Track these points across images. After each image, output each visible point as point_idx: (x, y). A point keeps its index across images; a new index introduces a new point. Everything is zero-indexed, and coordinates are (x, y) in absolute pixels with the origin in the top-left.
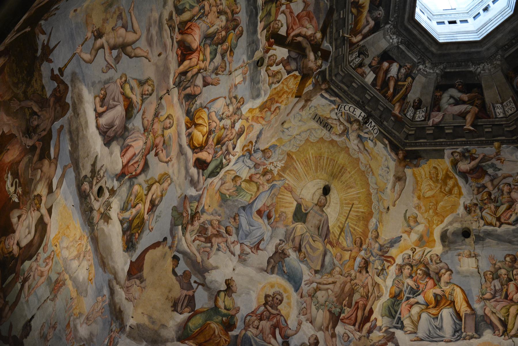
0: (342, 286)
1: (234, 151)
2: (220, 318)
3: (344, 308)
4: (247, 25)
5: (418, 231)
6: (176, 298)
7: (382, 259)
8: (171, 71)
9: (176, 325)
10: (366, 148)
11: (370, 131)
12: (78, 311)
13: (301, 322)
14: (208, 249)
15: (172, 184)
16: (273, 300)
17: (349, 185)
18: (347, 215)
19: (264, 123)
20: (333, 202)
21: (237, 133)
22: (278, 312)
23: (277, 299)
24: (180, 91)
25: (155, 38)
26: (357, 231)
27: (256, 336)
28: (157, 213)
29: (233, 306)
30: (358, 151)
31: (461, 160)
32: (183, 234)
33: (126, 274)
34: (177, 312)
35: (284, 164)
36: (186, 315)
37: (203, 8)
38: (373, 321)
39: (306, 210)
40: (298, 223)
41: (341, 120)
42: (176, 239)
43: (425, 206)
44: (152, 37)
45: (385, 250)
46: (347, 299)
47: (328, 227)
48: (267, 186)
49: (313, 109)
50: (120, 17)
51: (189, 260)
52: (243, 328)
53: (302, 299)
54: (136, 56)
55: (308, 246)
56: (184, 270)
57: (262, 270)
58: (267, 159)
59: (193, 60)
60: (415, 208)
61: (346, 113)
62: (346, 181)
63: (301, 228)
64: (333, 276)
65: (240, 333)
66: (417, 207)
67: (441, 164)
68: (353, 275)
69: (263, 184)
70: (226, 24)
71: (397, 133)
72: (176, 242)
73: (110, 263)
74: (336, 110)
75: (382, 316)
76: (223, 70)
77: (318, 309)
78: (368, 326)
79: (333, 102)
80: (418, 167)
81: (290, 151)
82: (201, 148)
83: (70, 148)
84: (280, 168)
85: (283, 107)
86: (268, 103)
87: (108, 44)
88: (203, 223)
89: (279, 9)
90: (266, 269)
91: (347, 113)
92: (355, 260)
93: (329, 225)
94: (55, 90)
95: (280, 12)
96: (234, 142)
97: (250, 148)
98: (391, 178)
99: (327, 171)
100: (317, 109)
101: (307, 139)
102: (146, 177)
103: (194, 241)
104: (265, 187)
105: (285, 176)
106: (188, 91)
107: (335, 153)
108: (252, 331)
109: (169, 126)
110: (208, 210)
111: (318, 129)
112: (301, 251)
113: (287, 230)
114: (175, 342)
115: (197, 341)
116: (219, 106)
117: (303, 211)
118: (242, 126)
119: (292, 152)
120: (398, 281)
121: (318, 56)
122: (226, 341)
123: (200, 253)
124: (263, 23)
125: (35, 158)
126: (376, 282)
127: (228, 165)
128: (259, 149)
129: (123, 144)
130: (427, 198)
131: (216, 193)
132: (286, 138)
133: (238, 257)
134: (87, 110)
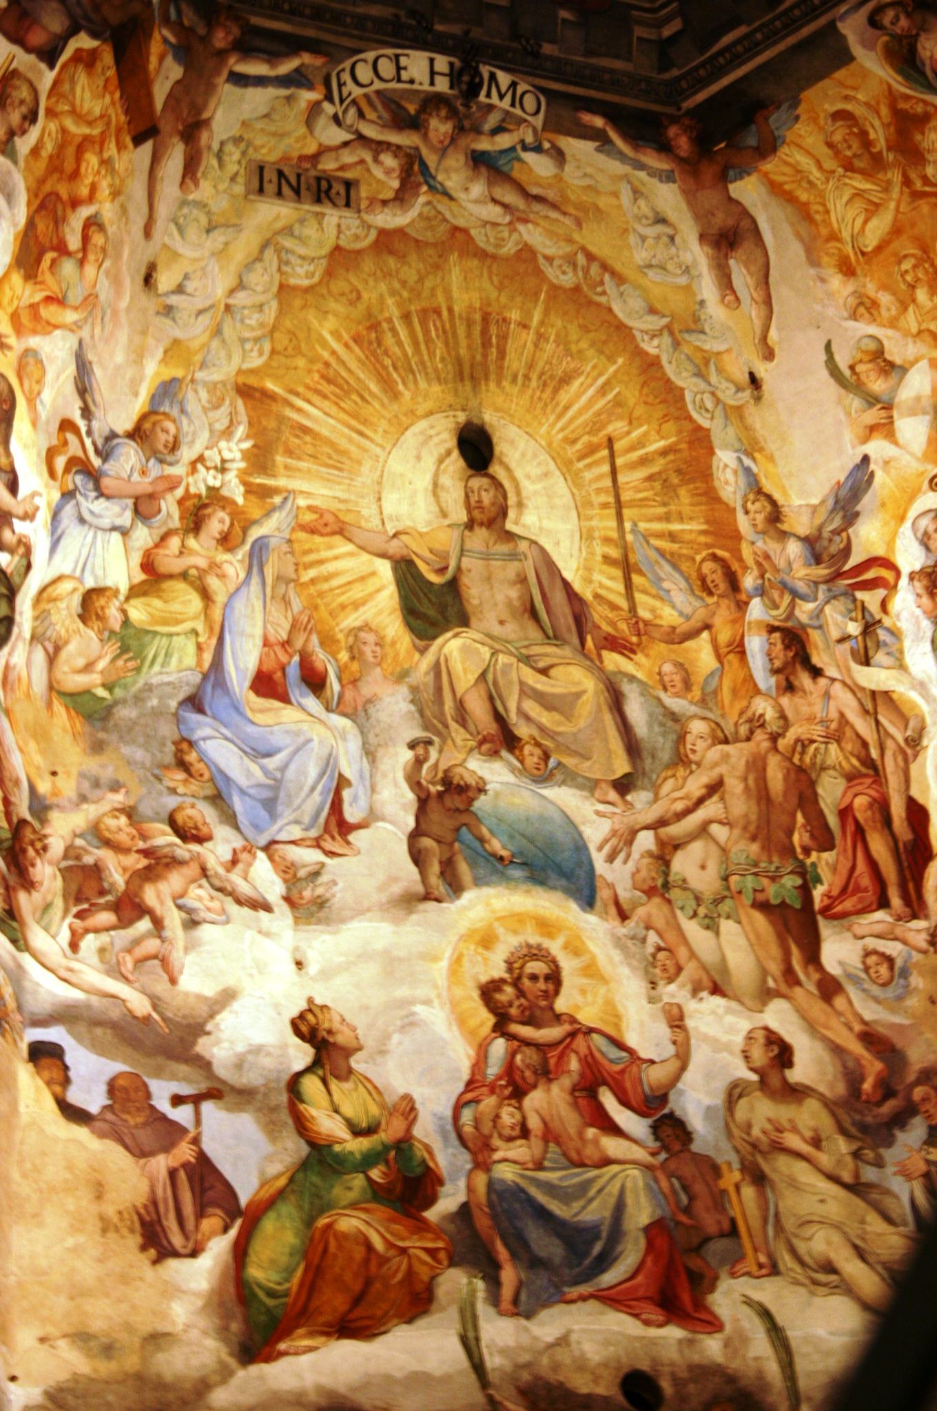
0: (751, 782)
2: (358, 1181)
3: (808, 862)
5: (918, 399)
6: (139, 1204)
7: (842, 589)
9: (205, 1307)
10: (535, 191)
11: (507, 113)
13: (675, 1011)
14: (152, 945)
16: (521, 993)
17: (552, 377)
18: (611, 500)
19: (70, 317)
20: (528, 477)
23: (534, 978)
26: (687, 537)
27: (539, 1166)
29: (383, 1106)
30: (508, 219)
31: (923, 28)
32: (14, 941)
34: (176, 1254)
35: (248, 437)
36: (218, 1248)
39: (442, 571)
40: (440, 640)
41: (370, 131)
43: (884, 287)
45: (834, 549)
46: (800, 818)
47: (566, 585)
48: (234, 564)
49: (233, 154)
51: (99, 1031)
53: (631, 923)
55: (531, 707)
57: (411, 901)
58: (169, 458)
60: (854, 316)
61: (374, 97)
62: (531, 366)
63: (465, 650)
64: (698, 764)
65: (470, 1189)
66: (862, 310)
67: (855, 88)
68: (770, 714)
69: (214, 566)
71: (618, 65)
74: (329, 109)
77: (711, 925)
79: (297, 80)
80: (773, 149)
81: (240, 372)
84: (243, 465)
85: (107, 210)
86: (41, 226)
88: (70, 851)
90: (420, 889)
91: (378, 92)
92: (743, 653)
93: (568, 575)
97: (74, 448)
98: (697, 255)
99: (436, 370)
100: (249, 144)
101: (282, 287)
103: (74, 946)
104: (230, 570)
105: (281, 482)
107: (421, 280)
108: (511, 1154)
111: (302, 221)
112: (519, 739)
113: (414, 690)
115: (322, 1319)
117: (434, 578)
122: (431, 1252)
123: (127, 980)
126: (873, 693)
127: (29, 566)
128: (113, 435)
130: (879, 249)
131: (49, 705)
132: (195, 331)
133: (285, 907)
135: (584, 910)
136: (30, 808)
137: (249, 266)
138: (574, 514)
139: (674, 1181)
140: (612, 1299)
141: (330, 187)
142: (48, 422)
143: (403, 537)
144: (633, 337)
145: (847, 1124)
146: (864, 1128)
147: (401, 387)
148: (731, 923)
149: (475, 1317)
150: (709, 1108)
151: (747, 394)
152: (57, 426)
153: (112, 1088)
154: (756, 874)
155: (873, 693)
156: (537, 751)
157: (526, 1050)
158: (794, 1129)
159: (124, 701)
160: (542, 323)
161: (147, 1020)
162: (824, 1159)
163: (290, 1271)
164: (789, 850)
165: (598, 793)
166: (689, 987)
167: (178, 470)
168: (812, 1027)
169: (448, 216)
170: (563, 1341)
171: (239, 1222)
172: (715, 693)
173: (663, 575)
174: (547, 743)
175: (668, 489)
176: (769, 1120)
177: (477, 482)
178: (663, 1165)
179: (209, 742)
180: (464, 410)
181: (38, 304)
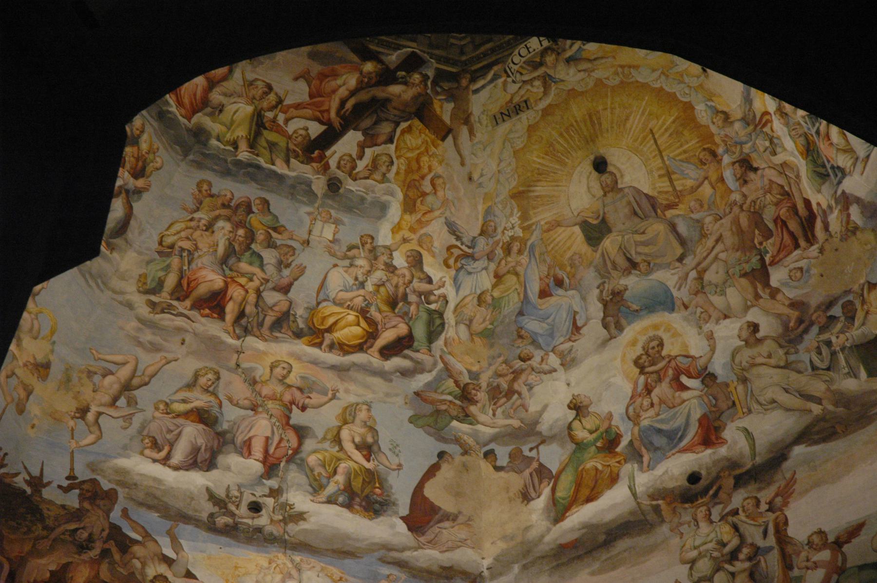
0: (734, 229)
1: (434, 283)
3: (762, 247)
4: (262, 189)
6: (521, 489)
8: (218, 335)
10: (592, 57)
13: (710, 333)
14: (519, 402)
19: (437, 213)
22: (667, 360)
23: (653, 348)
24: (258, 333)
25: (158, 339)
27: (658, 415)
32: (471, 424)
33: (410, 533)
34: (533, 499)
35: (518, 211)
36: (547, 491)
37: (182, 250)
38: (818, 211)
40: (602, 244)
42: (465, 437)
44: (151, 343)
45: (751, 117)
46: (757, 232)
47: (646, 195)
48: (524, 259)
50: (90, 374)
53: (690, 309)
54: (152, 376)
55: (641, 249)
56: (508, 453)
57: (604, 343)
59: (235, 294)
62: (612, 123)
65: (632, 434)
69: (518, 263)
70: (232, 223)
72: (471, 441)
73: (358, 545)
74: (509, 80)
75: (819, 191)
76: (291, 253)
77: (723, 293)
78: (819, 225)
81: (510, 190)
82: (372, 335)
83: (156, 515)
84: (519, 222)
85: (439, 169)
86: (411, 194)
87: (104, 405)
89: (279, 125)
90: (608, 337)
91: (524, 62)
93: (645, 192)
94: (80, 495)
95: (284, 126)
96: (419, 278)
97: (456, 252)
101: (514, 152)
102: (317, 437)
103: (494, 415)
104: (523, 261)
105: (534, 220)
106: (269, 321)
107: (562, 118)
108: (647, 416)
109: (285, 372)
113: (595, 267)
114: (554, 528)
117: (595, 222)
118: (409, 253)
119: (514, 188)
120: (793, 130)
121: (402, 78)
122: (618, 462)
123: (512, 418)
125: (117, 557)
127: (447, 302)
128: (474, 238)
131: (472, 340)
133: (562, 368)
134: (143, 472)
135: (670, 313)
136: (470, 379)
138: (644, 166)
139: (711, 397)
140: (684, 450)
141: (520, 106)
142: (440, 252)
143: (582, 214)
144: (649, 86)
145: (784, 343)
146: (790, 341)
147: (567, 160)
148: (731, 288)
149: (634, 477)
150: (724, 364)
151: (703, 77)
153: (510, 456)
154: (740, 264)
155: (781, 164)
158: (760, 355)
159: (498, 326)
160: (612, 103)
161: (520, 427)
162: (773, 361)
163: (570, 489)
164: (755, 247)
165: (671, 267)
166: (715, 321)
167: (499, 237)
168: (766, 312)
169: (565, 88)
170: (667, 471)
171: (553, 480)
172: (714, 202)
174: (649, 259)
175: (678, 133)
176: (749, 357)
178: (705, 394)
180: (592, 154)
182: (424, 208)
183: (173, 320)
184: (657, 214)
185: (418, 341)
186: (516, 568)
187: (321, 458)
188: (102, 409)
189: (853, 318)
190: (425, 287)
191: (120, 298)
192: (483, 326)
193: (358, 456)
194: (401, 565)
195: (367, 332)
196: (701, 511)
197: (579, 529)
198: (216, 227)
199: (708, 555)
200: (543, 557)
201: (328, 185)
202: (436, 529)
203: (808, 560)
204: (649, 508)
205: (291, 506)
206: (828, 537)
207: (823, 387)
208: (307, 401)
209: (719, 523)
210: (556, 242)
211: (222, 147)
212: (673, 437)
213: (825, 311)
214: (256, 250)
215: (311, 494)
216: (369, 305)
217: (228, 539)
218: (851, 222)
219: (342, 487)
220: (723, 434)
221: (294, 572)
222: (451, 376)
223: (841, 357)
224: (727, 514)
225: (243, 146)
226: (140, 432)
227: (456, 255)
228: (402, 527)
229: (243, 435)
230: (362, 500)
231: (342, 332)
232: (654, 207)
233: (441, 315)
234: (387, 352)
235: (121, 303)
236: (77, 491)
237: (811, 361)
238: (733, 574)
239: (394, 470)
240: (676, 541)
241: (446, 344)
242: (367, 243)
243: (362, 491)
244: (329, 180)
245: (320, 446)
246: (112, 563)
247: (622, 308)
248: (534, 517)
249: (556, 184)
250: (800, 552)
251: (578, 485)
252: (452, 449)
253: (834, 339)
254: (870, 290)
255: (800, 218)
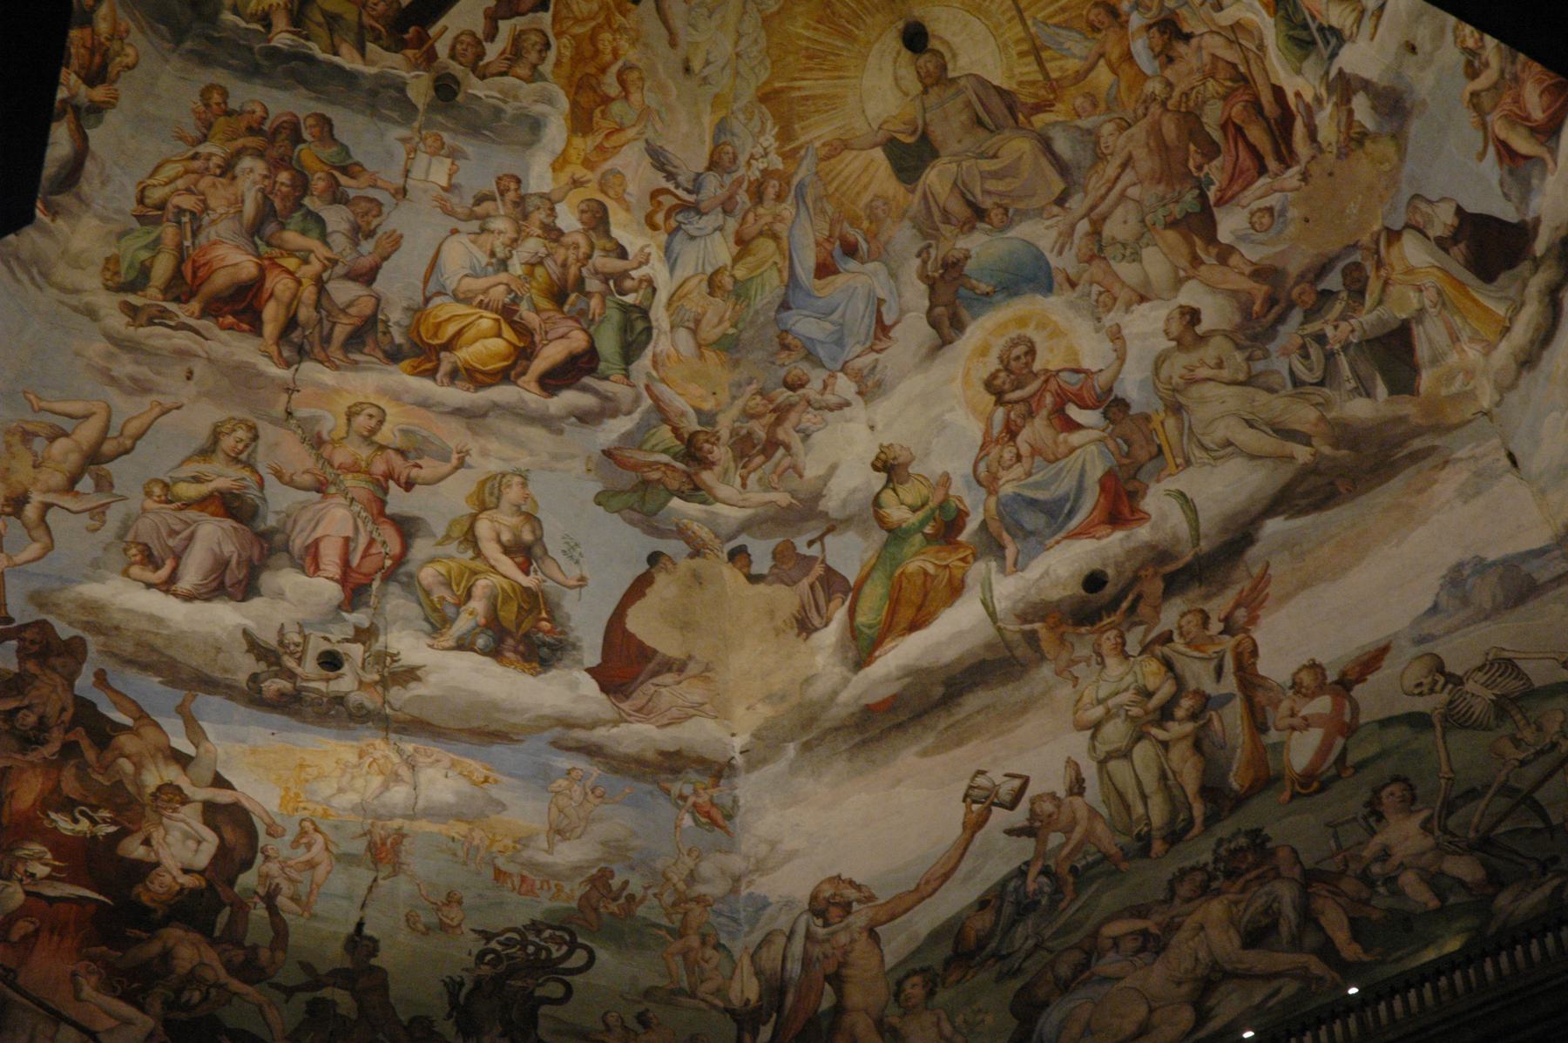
0: (1152, 144)
3: (1202, 175)
4: (318, 99)
12: (509, 842)
13: (1115, 329)
14: (787, 461)
15: (531, 476)
18: (1014, 13)
19: (631, 133)
21: (585, 232)
22: (1043, 378)
23: (1018, 358)
24: (322, 356)
25: (143, 372)
27: (1029, 474)
28: (553, 544)
32: (704, 502)
33: (603, 696)
34: (816, 629)
35: (775, 124)
36: (840, 615)
37: (181, 211)
38: (1297, 107)
42: (695, 526)
44: (134, 379)
46: (1192, 147)
47: (998, 89)
48: (787, 209)
50: (27, 436)
51: (764, 526)
52: (984, 497)
53: (1079, 289)
55: (991, 185)
56: (771, 550)
58: (734, 168)
59: (279, 288)
65: (985, 510)
69: (778, 218)
70: (267, 162)
72: (704, 533)
73: (514, 719)
75: (1299, 72)
77: (1136, 257)
78: (1299, 128)
81: (758, 89)
82: (524, 353)
85: (631, 54)
86: (583, 100)
87: (55, 491)
88: (734, 432)
93: (996, 83)
94: (18, 651)
96: (604, 249)
97: (668, 201)
101: (764, 20)
102: (434, 536)
103: (744, 485)
104: (786, 214)
105: (803, 139)
106: (340, 333)
108: (1010, 477)
109: (373, 423)
110: (718, 405)
113: (913, 219)
114: (855, 678)
116: (460, 256)
117: (910, 140)
118: (583, 206)
119: (765, 83)
122: (963, 560)
123: (775, 489)
124: (345, 49)
125: (90, 755)
127: (654, 290)
128: (699, 175)
129: (292, 557)
131: (701, 356)
134: (130, 605)
136: (700, 423)
137: (740, 21)
138: (992, 39)
139: (1119, 440)
140: (1076, 535)
143: (885, 127)
146: (1255, 338)
147: (857, 32)
148: (1151, 249)
149: (990, 584)
152: (648, 198)
153: (775, 555)
155: (1232, 26)
156: (1001, 210)
157: (1017, 407)
158: (1203, 363)
162: (1225, 374)
167: (741, 172)
168: (1212, 288)
170: (1046, 573)
171: (850, 595)
172: (1116, 98)
173: (1062, 40)
174: (1006, 201)
177: (926, 61)
178: (1110, 435)
179: (798, 325)
181: (601, 143)
182: (607, 125)
183: (169, 338)
184: (1017, 122)
185: (606, 361)
186: (791, 750)
187: (443, 572)
188: (50, 498)
189: (1361, 293)
190: (615, 264)
191: (73, 300)
192: (719, 331)
193: (507, 565)
194: (591, 751)
195: (515, 347)
196: (1108, 639)
197: (898, 679)
198: (238, 170)
199: (1122, 713)
200: (837, 729)
201: (436, 89)
202: (649, 688)
203: (1293, 715)
204: (1018, 636)
205: (394, 657)
206: (1328, 673)
207: (1312, 414)
208: (415, 472)
209: (1139, 658)
210: (841, 178)
211: (243, 24)
212: (1056, 514)
213: (1313, 283)
214: (311, 208)
215: (429, 635)
216: (516, 300)
217: (285, 719)
218: (1355, 124)
219: (482, 621)
220: (1142, 503)
221: (404, 772)
222: (666, 420)
223: (1343, 361)
224: (1153, 642)
225: (280, 22)
226: (121, 537)
227: (666, 208)
228: (590, 687)
229: (305, 534)
230: (519, 643)
231: (472, 349)
232: (1012, 109)
233: (644, 313)
234: (552, 381)
235: (75, 309)
236: (14, 643)
237: (1292, 372)
238: (1165, 745)
239: (571, 588)
240: (1065, 692)
241: (655, 363)
242: (508, 190)
243: (519, 626)
244: (437, 80)
245: (440, 551)
246: (83, 767)
247: (962, 291)
248: (820, 660)
249: (836, 74)
250: (1280, 701)
251: (895, 601)
252: (673, 547)
253: (1329, 331)
254: (1389, 243)
255: (1266, 119)
